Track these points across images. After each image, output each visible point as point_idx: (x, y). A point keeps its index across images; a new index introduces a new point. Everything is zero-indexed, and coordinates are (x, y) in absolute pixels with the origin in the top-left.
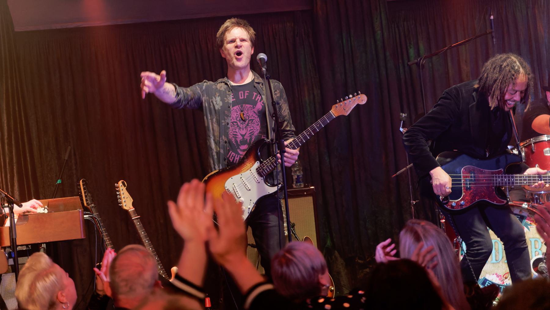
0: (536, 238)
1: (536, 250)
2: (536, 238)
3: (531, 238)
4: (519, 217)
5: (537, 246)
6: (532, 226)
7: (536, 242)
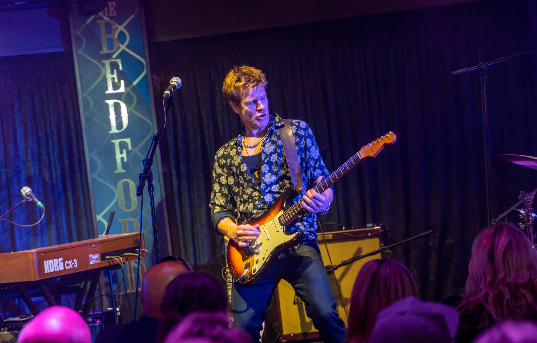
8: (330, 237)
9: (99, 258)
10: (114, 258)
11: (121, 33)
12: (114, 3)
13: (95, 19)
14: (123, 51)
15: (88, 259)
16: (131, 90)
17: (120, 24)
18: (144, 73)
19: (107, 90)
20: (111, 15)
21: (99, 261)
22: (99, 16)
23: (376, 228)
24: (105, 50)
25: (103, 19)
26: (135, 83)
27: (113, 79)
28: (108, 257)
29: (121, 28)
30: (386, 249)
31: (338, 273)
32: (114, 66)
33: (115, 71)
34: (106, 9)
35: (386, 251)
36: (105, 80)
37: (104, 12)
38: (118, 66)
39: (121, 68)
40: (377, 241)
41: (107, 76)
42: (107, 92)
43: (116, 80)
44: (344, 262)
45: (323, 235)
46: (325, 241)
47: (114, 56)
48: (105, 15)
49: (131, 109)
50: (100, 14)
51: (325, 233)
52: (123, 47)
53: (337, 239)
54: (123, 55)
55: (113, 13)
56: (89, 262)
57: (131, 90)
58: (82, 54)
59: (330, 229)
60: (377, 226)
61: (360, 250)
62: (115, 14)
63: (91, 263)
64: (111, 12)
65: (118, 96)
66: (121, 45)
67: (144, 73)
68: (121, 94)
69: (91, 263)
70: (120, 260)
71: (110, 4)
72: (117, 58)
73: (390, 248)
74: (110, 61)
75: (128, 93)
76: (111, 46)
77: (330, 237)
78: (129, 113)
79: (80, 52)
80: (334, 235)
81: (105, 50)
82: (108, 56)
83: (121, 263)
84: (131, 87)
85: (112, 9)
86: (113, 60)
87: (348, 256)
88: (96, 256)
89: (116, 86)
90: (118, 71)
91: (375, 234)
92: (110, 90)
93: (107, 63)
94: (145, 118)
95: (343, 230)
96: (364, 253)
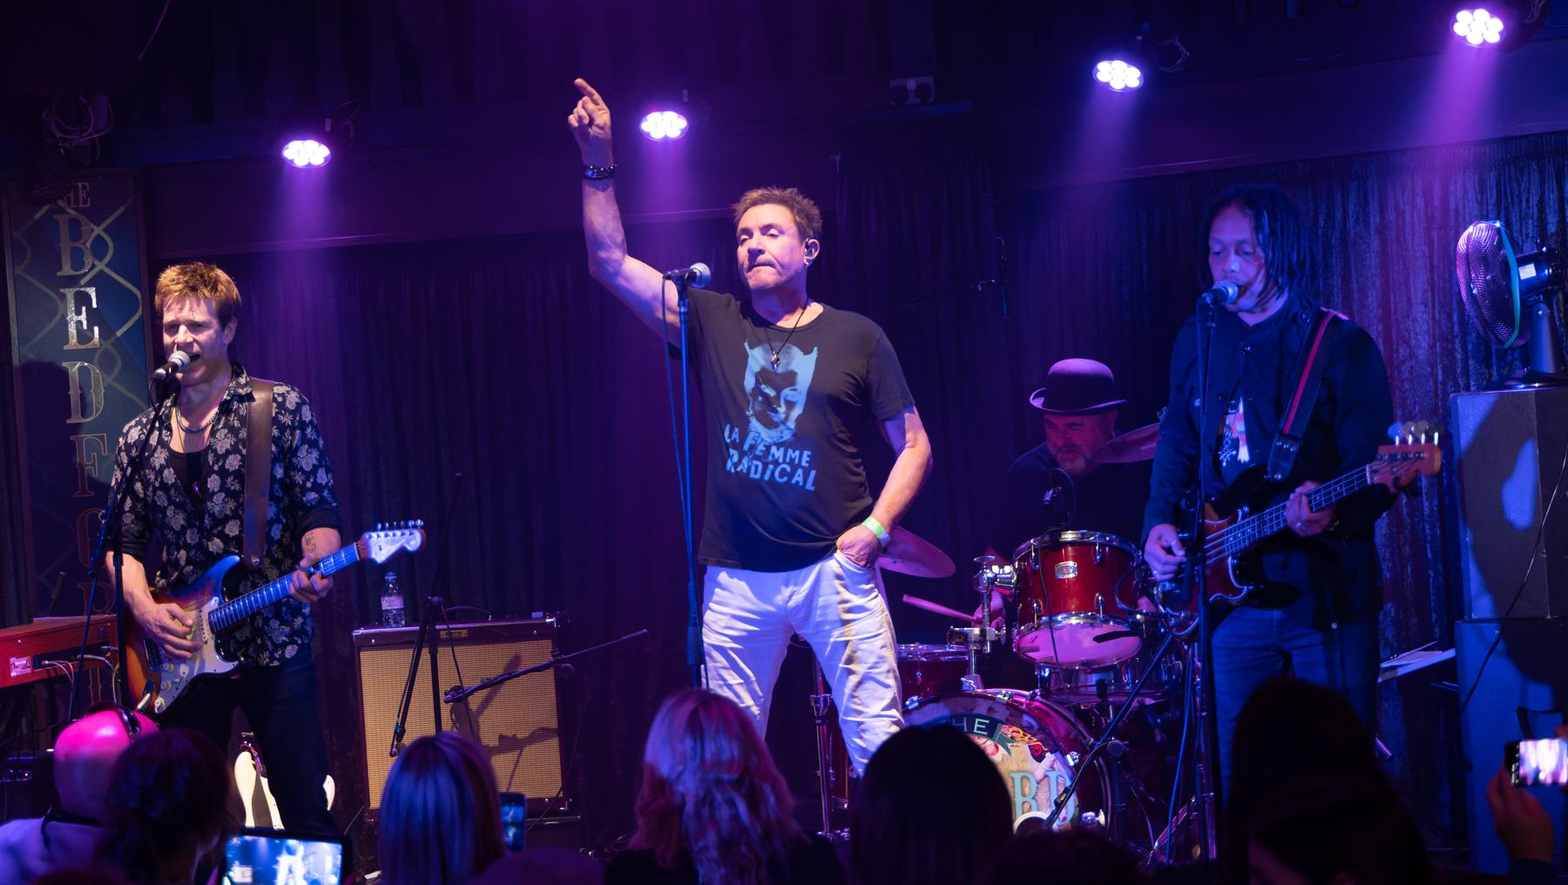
0: (1025, 771)
1: (1024, 799)
2: (1025, 771)
3: (1013, 772)
4: (987, 722)
5: (1027, 791)
6: (1015, 744)
7: (1025, 781)
8: (464, 633)
9: (28, 665)
10: (59, 665)
11: (99, 236)
12: (87, 184)
13: (49, 210)
14: (101, 272)
15: (7, 667)
16: (113, 345)
17: (98, 225)
18: (140, 312)
19: (67, 341)
20: (81, 205)
21: (29, 670)
22: (57, 205)
23: (548, 620)
24: (67, 270)
25: (67, 213)
26: (119, 333)
27: (79, 323)
28: (47, 662)
29: (98, 230)
30: (564, 661)
31: (474, 701)
32: (83, 299)
33: (84, 309)
34: (71, 195)
35: (563, 665)
36: (65, 324)
37: (69, 198)
38: (91, 300)
39: (95, 305)
40: (547, 645)
41: (68, 318)
42: (65, 348)
43: (85, 327)
44: (486, 681)
45: (449, 629)
46: (453, 642)
47: (83, 282)
48: (69, 205)
49: (110, 380)
50: (60, 202)
51: (451, 626)
52: (101, 266)
53: (477, 638)
54: (99, 281)
55: (85, 202)
56: (10, 672)
57: (113, 345)
58: (23, 274)
59: (465, 618)
60: (550, 618)
61: (516, 660)
62: (88, 205)
63: (13, 674)
64: (81, 200)
65: (86, 355)
66: (97, 262)
67: (140, 312)
68: (94, 350)
69: (13, 674)
70: (67, 667)
71: (80, 185)
72: (89, 284)
73: (571, 660)
74: (78, 289)
75: (106, 351)
76: (78, 263)
77: (464, 633)
78: (108, 388)
79: (19, 270)
80: (472, 632)
81: (67, 270)
82: (72, 281)
83: (71, 674)
84: (113, 339)
85: (82, 195)
86: (82, 289)
87: (496, 671)
88: (23, 661)
89: (84, 336)
90: (90, 310)
91: (544, 632)
92: (73, 340)
93: (70, 293)
94: (134, 397)
95: (488, 621)
96: (520, 669)
